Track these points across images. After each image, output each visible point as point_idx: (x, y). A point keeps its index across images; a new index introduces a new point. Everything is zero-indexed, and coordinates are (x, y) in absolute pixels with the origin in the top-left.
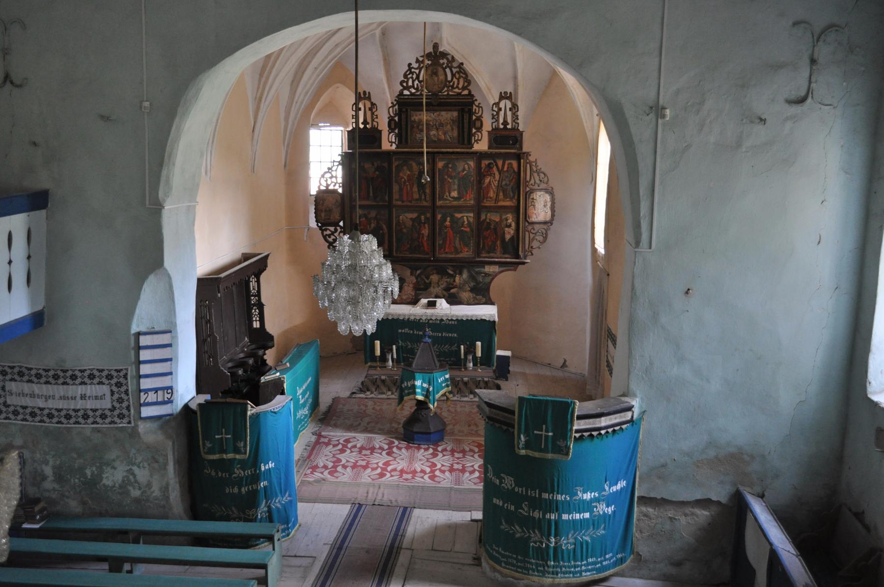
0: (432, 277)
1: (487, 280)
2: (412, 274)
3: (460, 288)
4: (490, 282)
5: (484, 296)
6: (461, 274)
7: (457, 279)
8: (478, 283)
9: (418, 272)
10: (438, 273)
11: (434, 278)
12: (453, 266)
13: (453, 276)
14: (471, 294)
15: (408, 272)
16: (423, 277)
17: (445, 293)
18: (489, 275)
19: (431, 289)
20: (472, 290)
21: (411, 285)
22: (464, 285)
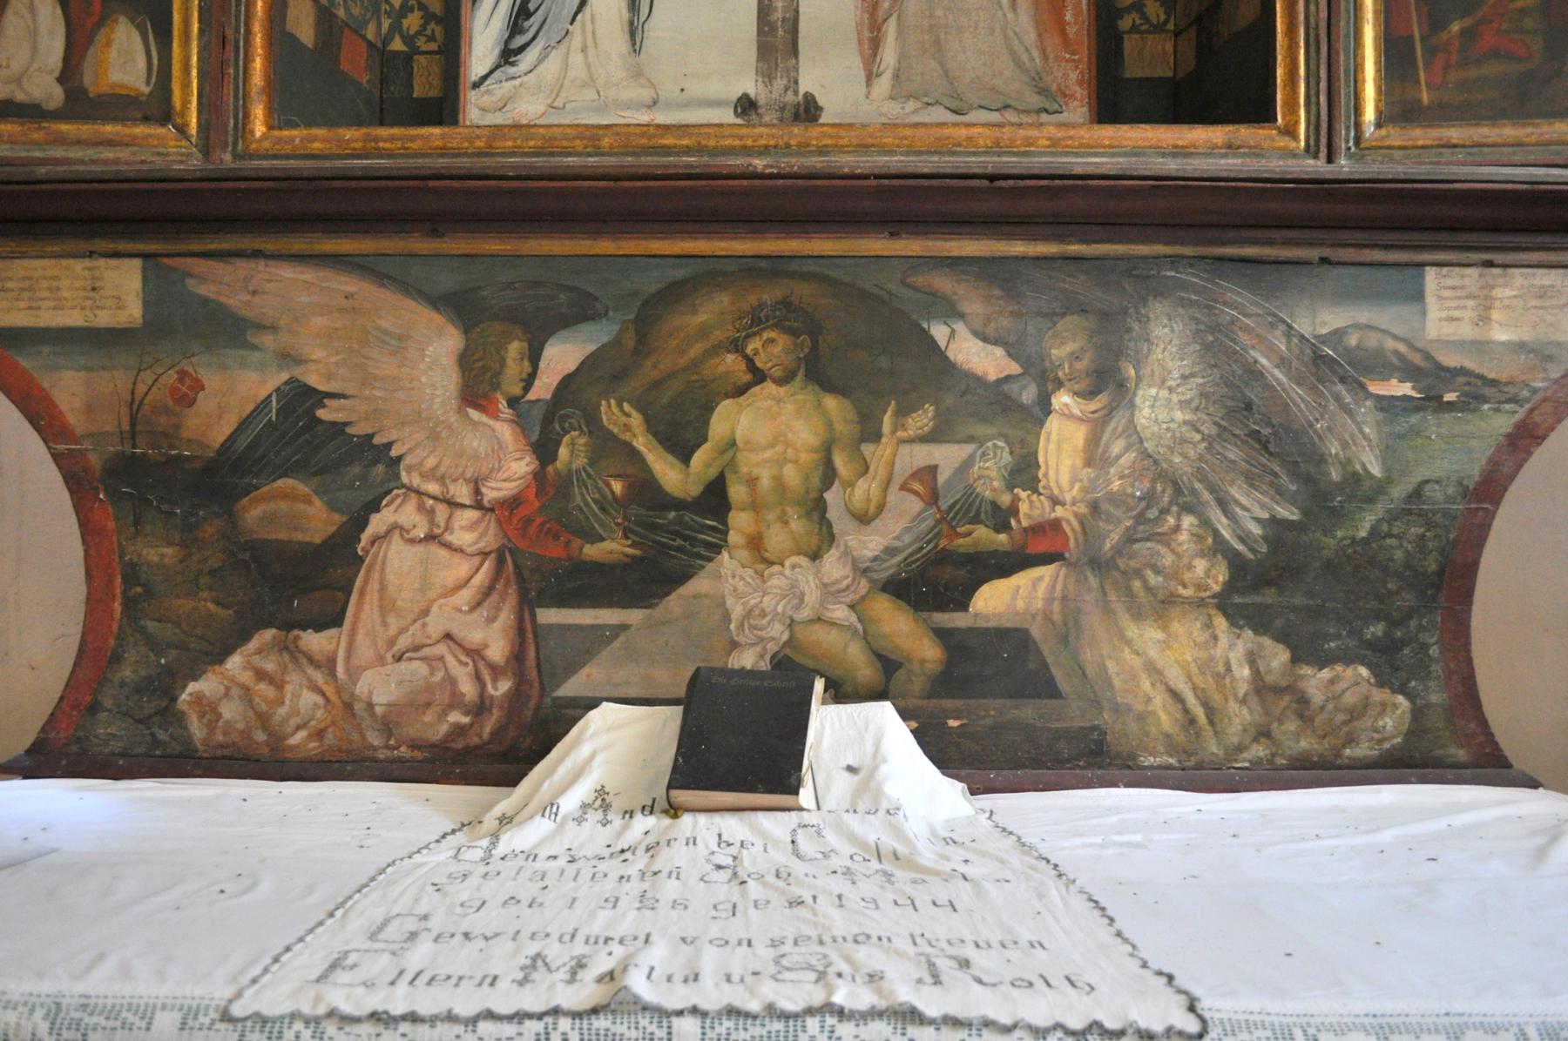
0: (727, 420)
1: (1453, 452)
2: (477, 388)
3: (1100, 565)
4: (1489, 490)
5: (1390, 664)
6: (1107, 380)
7: (1062, 444)
8: (1325, 498)
9: (563, 355)
10: (817, 371)
11: (769, 429)
12: (985, 269)
13: (1014, 412)
14: (1235, 649)
15: (438, 349)
16: (623, 419)
17: (900, 627)
18: (1478, 391)
19: (728, 580)
20: (1260, 587)
21: (467, 531)
22: (1146, 523)
